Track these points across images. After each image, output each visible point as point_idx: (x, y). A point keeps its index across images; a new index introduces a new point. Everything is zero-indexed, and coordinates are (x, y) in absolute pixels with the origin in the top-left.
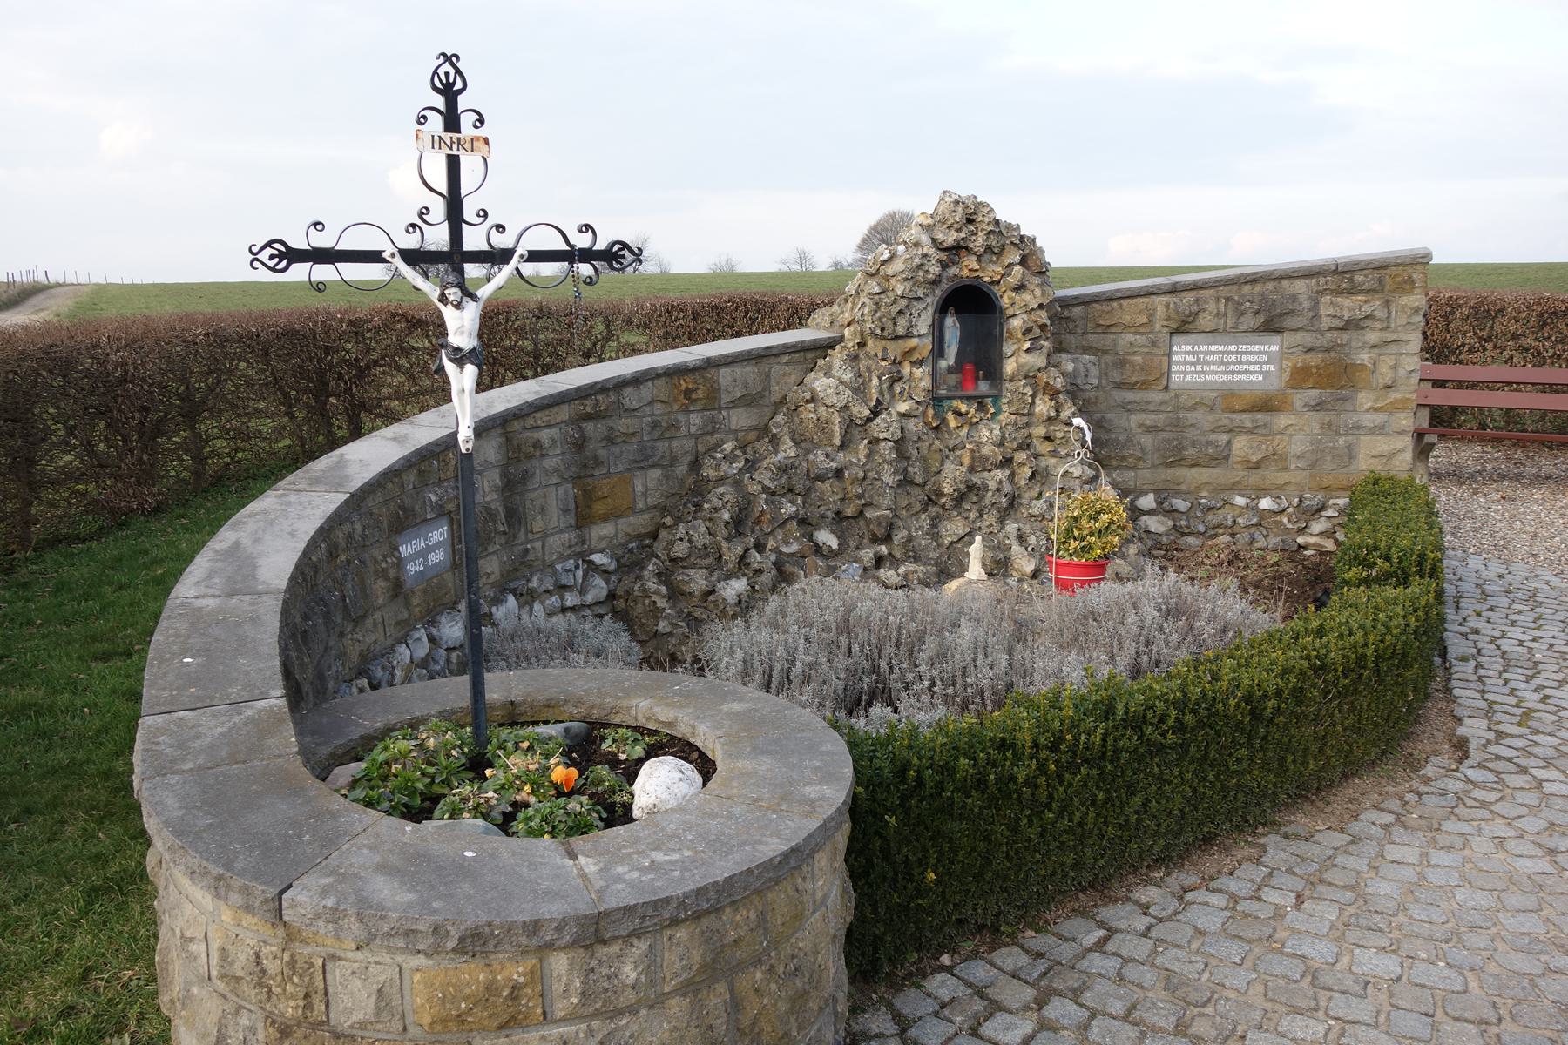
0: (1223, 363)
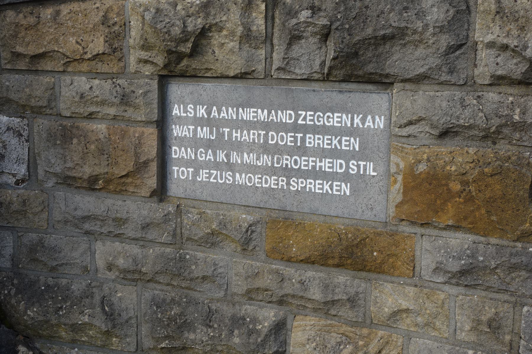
0: (266, 148)
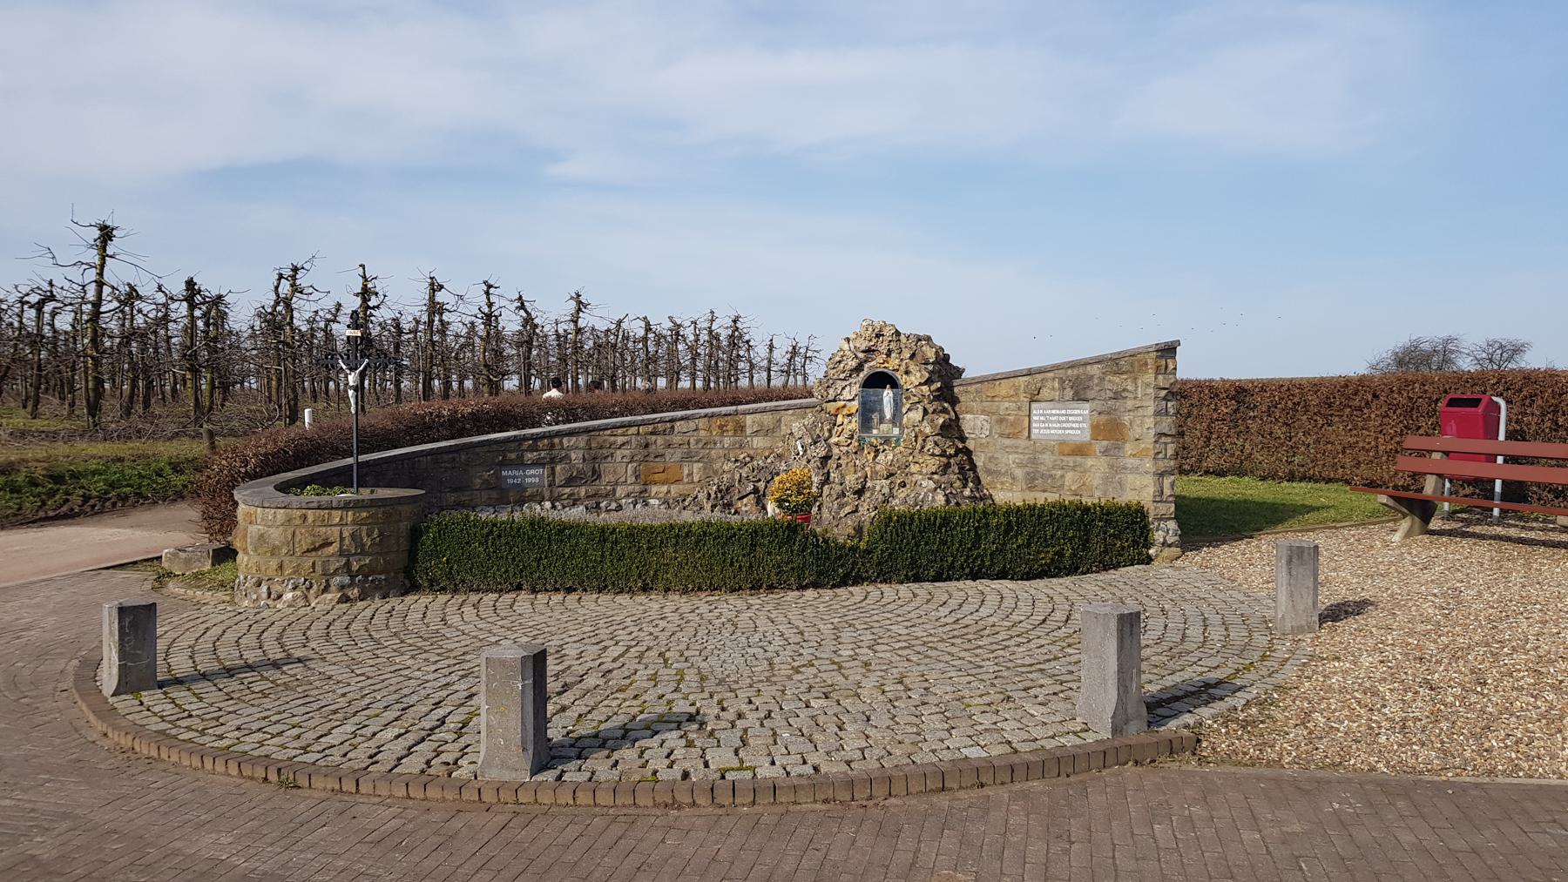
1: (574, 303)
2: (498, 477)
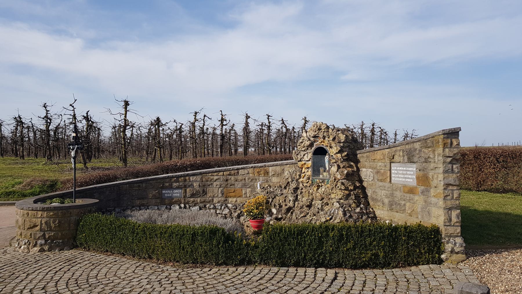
0: (403, 174)
1: (303, 121)
2: (161, 194)
